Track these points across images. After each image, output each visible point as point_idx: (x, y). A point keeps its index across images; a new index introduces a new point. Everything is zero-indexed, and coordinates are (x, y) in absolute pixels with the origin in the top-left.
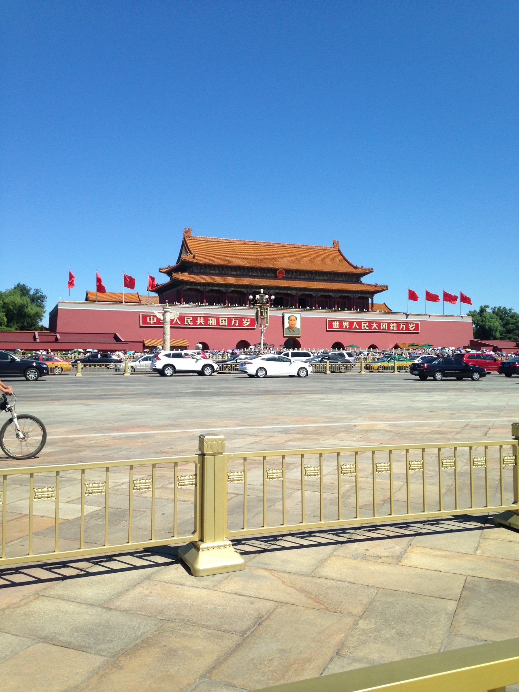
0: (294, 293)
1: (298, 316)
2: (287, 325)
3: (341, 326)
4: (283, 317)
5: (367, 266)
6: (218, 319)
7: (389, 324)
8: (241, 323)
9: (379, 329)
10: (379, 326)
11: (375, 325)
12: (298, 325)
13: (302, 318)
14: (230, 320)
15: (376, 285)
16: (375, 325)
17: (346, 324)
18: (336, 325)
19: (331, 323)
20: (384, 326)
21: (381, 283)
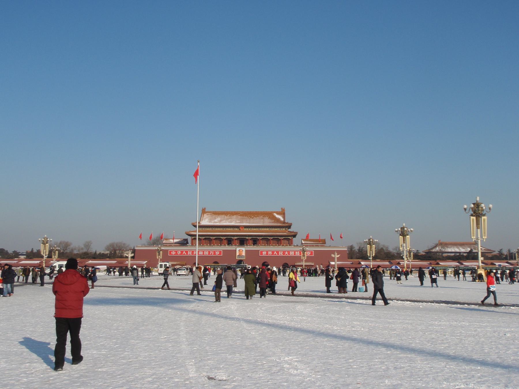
0: (247, 238)
1: (244, 249)
2: (238, 254)
3: (267, 253)
4: (236, 250)
5: (290, 222)
6: (203, 252)
7: (295, 252)
8: (215, 254)
9: (289, 254)
10: (289, 254)
11: (286, 253)
12: (244, 254)
13: (246, 251)
14: (209, 252)
15: (293, 232)
16: (286, 253)
17: (270, 253)
18: (264, 253)
19: (261, 252)
20: (292, 253)
21: (295, 231)
